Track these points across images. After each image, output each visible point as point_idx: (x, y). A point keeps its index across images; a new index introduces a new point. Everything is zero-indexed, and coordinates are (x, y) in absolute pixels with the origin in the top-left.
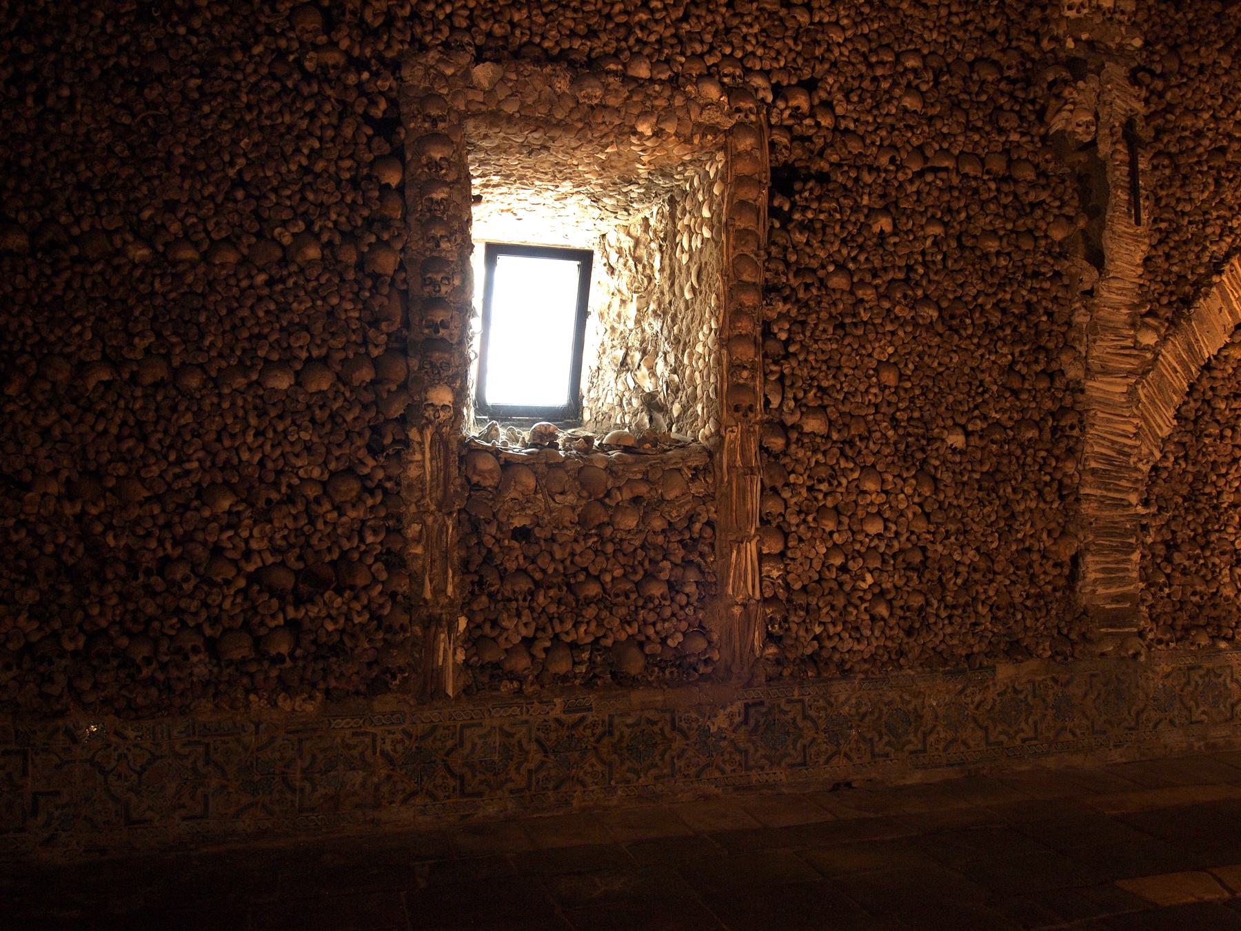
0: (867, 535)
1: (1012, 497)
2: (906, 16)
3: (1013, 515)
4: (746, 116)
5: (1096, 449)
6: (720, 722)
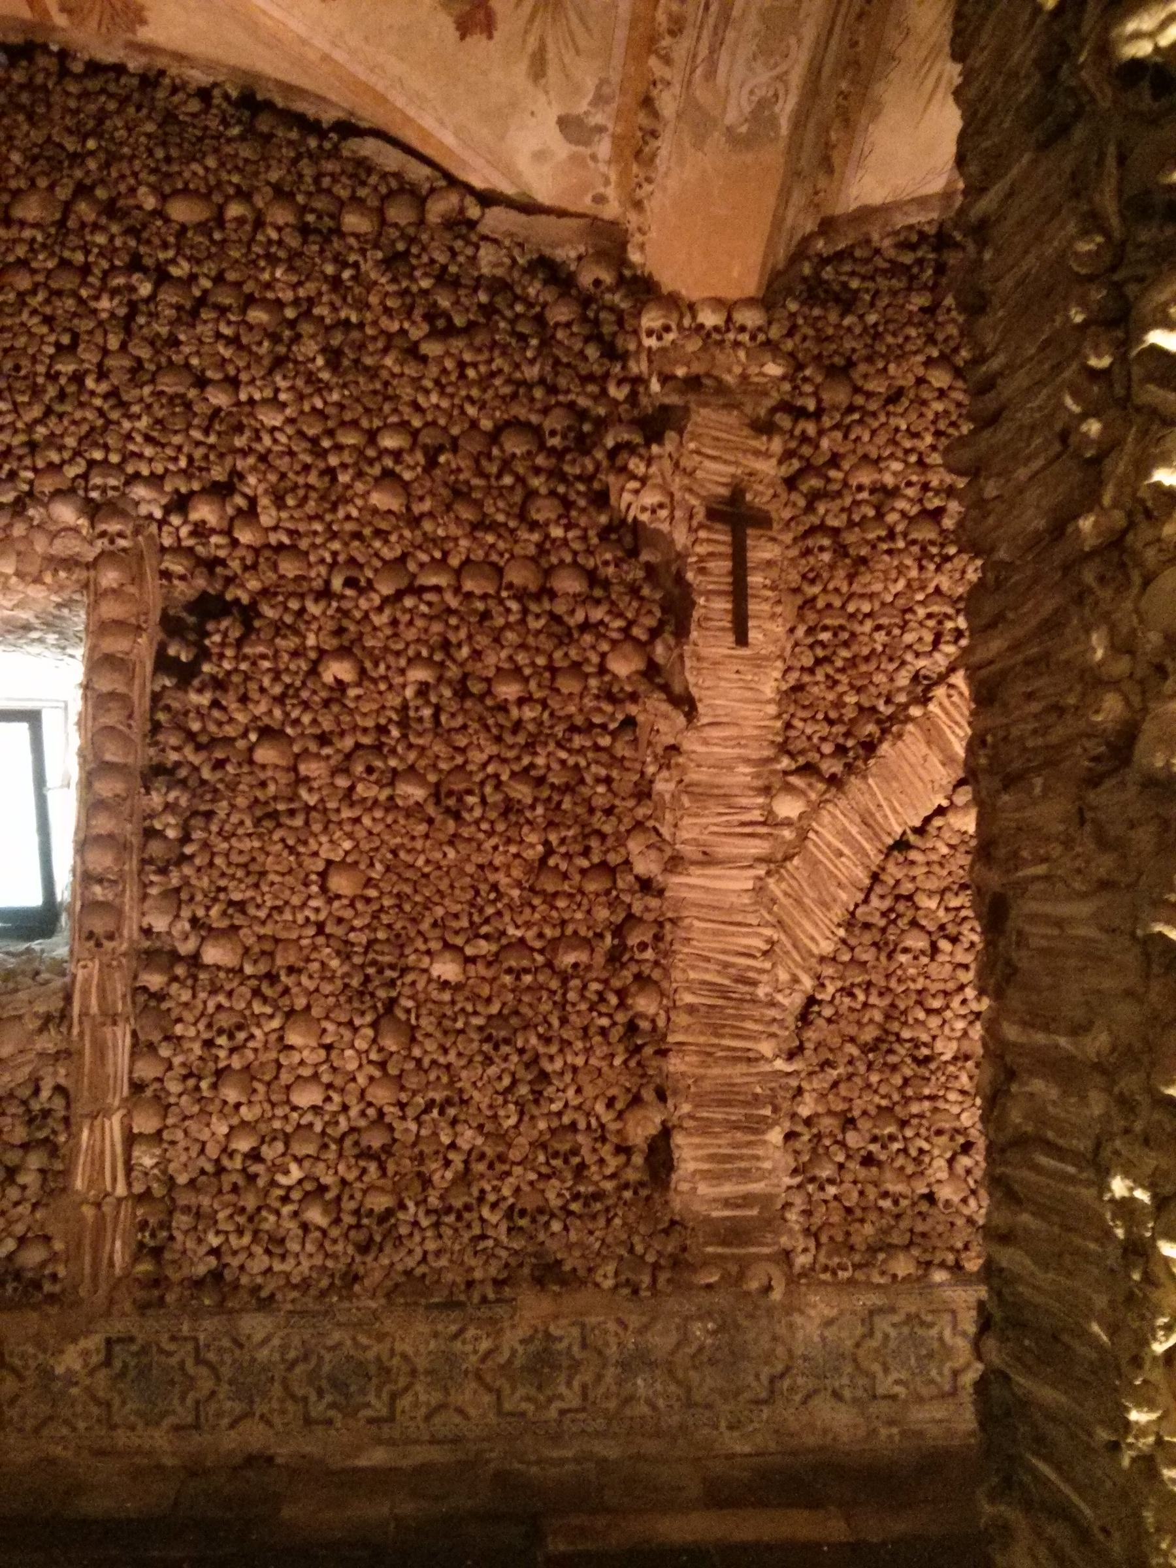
0: (295, 1108)
1: (542, 1050)
2: (394, 375)
3: (544, 1076)
4: (112, 542)
5: (692, 975)
6: (70, 1360)
